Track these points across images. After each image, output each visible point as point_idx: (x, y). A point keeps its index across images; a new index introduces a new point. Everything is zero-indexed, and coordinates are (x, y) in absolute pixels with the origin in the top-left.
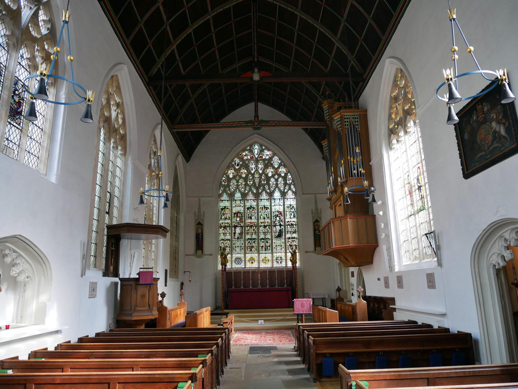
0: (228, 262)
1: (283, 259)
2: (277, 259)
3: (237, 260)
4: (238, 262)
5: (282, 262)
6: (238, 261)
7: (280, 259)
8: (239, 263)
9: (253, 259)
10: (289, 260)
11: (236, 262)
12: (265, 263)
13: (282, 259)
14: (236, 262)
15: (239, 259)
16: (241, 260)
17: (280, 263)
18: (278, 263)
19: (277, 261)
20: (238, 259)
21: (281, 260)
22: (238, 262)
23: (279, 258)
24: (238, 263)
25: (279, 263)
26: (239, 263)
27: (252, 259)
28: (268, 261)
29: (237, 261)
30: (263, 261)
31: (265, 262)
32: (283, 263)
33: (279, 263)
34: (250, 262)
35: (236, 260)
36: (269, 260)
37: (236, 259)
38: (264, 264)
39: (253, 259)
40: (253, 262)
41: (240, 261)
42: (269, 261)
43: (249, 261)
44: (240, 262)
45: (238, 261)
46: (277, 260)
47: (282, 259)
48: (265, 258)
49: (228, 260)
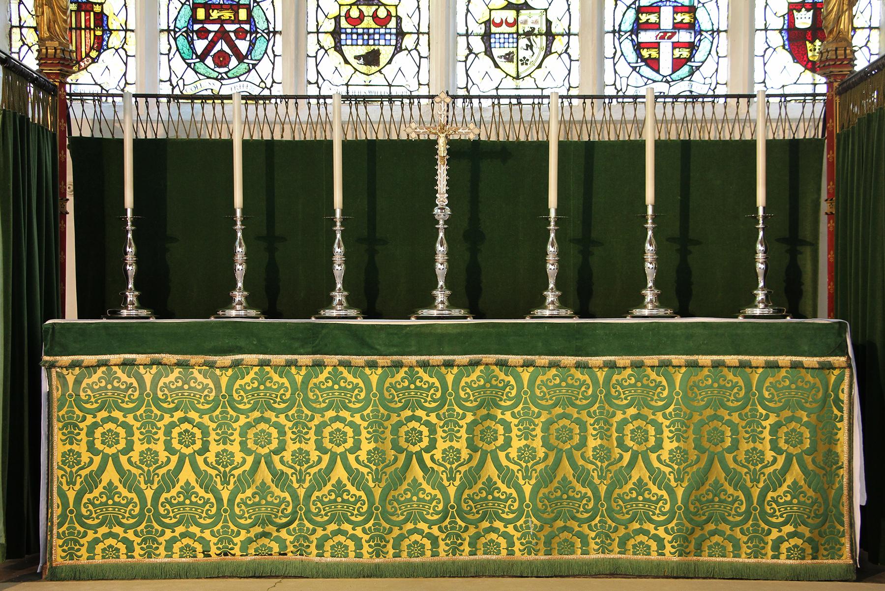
0: (115, 40)
1: (704, 23)
2: (638, 27)
3: (208, 20)
4: (222, 46)
5: (699, 56)
6: (222, 35)
7: (678, 26)
8: (234, 62)
9: (383, 23)
10: (777, 39)
11: (200, 45)
12: (510, 68)
13: (692, 26)
14: (200, 45)
15: (227, 15)
16: (250, 19)
17: (678, 64)
18: (653, 64)
19: (638, 47)
20: (215, 15)
21: (684, 36)
22: (222, 46)
23: (667, 13)
24: (222, 60)
25: (666, 66)
26: (234, 62)
27: (368, 22)
28: (540, 42)
29: (203, 34)
30: (487, 37)
31: (509, 57)
32: (708, 69)
33: (666, 66)
34: (351, 52)
35: (194, 19)
36: (550, 36)
37: (201, 14)
38: (497, 74)
39: (383, 23)
40: (386, 53)
41: (241, 34)
42: (559, 44)
43: (336, 33)
44: (243, 46)
45: (222, 35)
46: (646, 37)
47: (692, 26)
48: (509, 6)
49: (113, 24)
